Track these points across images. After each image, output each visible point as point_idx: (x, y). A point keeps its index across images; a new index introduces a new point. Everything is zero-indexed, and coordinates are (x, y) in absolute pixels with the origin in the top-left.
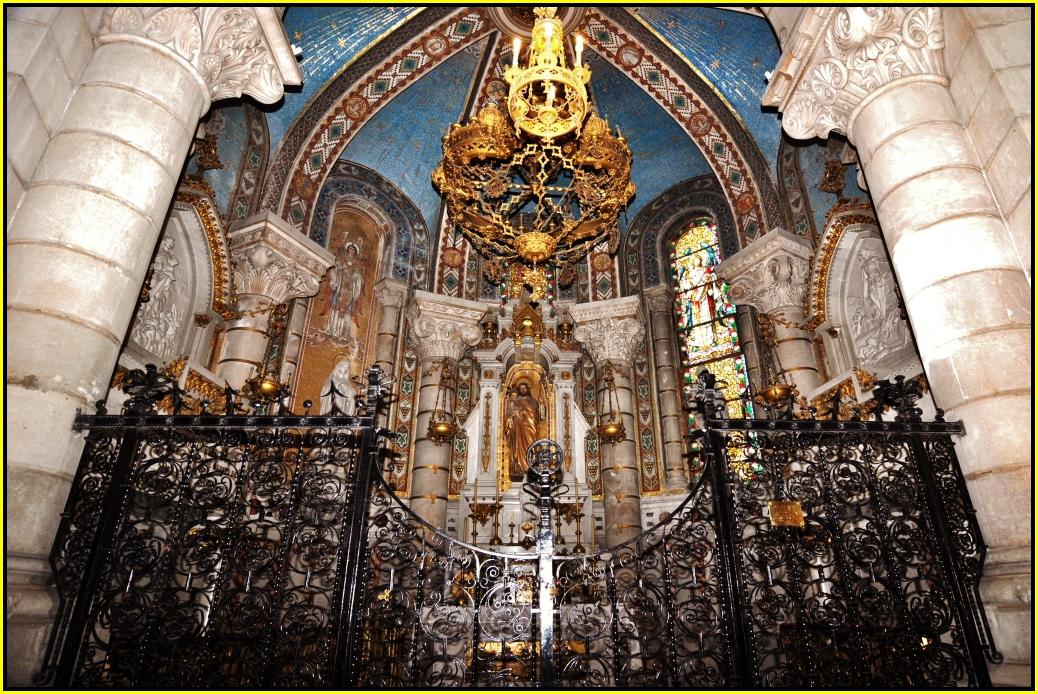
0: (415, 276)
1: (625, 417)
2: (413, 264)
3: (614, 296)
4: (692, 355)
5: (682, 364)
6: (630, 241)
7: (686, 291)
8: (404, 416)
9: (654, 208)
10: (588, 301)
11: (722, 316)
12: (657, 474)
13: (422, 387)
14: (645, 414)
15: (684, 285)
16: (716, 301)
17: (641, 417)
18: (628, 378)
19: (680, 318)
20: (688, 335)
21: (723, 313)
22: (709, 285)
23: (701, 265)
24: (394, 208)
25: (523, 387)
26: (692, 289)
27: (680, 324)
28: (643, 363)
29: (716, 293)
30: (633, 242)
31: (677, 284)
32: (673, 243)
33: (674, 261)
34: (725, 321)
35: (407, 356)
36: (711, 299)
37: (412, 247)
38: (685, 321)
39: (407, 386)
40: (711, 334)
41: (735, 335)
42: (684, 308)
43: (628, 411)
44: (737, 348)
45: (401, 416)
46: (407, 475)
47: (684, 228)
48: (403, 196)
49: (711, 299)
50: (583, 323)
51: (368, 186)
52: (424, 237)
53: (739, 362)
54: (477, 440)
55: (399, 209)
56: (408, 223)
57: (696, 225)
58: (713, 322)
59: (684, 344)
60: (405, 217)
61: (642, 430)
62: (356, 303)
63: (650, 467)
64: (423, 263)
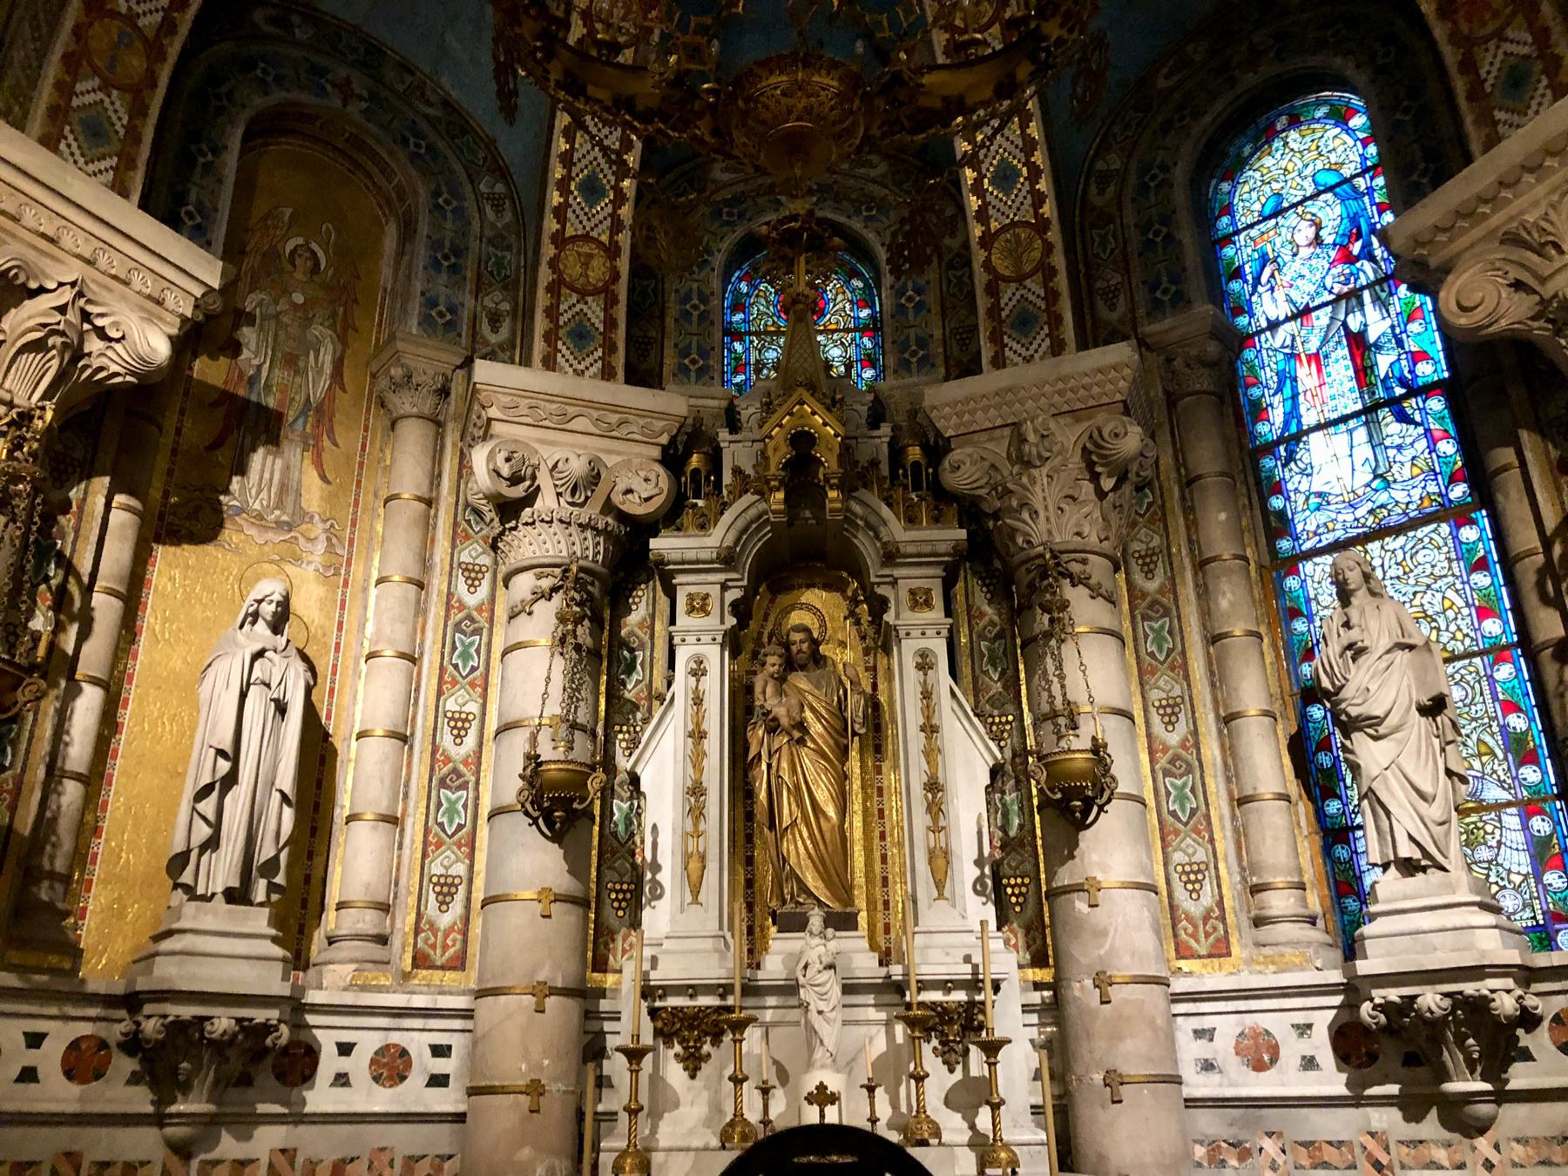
0: (485, 328)
1: (1113, 722)
2: (477, 293)
3: (1057, 348)
4: (1307, 522)
5: (1273, 551)
6: (1093, 189)
7: (1273, 325)
8: (459, 738)
9: (1161, 83)
10: (980, 371)
11: (1399, 391)
12: (1220, 903)
13: (504, 654)
14: (1170, 712)
15: (1269, 306)
16: (1378, 347)
17: (1156, 719)
18: (1111, 600)
19: (1259, 411)
20: (1291, 457)
21: (1402, 382)
22: (1352, 298)
24: (419, 135)
25: (796, 637)
26: (1293, 317)
27: (1262, 428)
28: (1151, 553)
29: (1376, 323)
30: (1101, 192)
31: (1241, 309)
32: (1225, 186)
33: (1228, 240)
34: (1411, 405)
35: (465, 557)
36: (1359, 344)
37: (474, 245)
38: (1277, 416)
39: (467, 647)
40: (1364, 451)
41: (1448, 447)
42: (1268, 376)
43: (1119, 703)
44: (1459, 491)
45: (446, 740)
46: (466, 920)
47: (1256, 139)
48: (446, 104)
49: (1359, 344)
50: (966, 436)
51: (342, 72)
52: (508, 217)
53: (1468, 534)
54: (669, 799)
55: (432, 136)
56: (464, 177)
57: (1295, 122)
58: (1369, 411)
59: (1278, 488)
60: (452, 159)
61: (1163, 761)
62: (319, 410)
63: (1194, 876)
64: (505, 288)
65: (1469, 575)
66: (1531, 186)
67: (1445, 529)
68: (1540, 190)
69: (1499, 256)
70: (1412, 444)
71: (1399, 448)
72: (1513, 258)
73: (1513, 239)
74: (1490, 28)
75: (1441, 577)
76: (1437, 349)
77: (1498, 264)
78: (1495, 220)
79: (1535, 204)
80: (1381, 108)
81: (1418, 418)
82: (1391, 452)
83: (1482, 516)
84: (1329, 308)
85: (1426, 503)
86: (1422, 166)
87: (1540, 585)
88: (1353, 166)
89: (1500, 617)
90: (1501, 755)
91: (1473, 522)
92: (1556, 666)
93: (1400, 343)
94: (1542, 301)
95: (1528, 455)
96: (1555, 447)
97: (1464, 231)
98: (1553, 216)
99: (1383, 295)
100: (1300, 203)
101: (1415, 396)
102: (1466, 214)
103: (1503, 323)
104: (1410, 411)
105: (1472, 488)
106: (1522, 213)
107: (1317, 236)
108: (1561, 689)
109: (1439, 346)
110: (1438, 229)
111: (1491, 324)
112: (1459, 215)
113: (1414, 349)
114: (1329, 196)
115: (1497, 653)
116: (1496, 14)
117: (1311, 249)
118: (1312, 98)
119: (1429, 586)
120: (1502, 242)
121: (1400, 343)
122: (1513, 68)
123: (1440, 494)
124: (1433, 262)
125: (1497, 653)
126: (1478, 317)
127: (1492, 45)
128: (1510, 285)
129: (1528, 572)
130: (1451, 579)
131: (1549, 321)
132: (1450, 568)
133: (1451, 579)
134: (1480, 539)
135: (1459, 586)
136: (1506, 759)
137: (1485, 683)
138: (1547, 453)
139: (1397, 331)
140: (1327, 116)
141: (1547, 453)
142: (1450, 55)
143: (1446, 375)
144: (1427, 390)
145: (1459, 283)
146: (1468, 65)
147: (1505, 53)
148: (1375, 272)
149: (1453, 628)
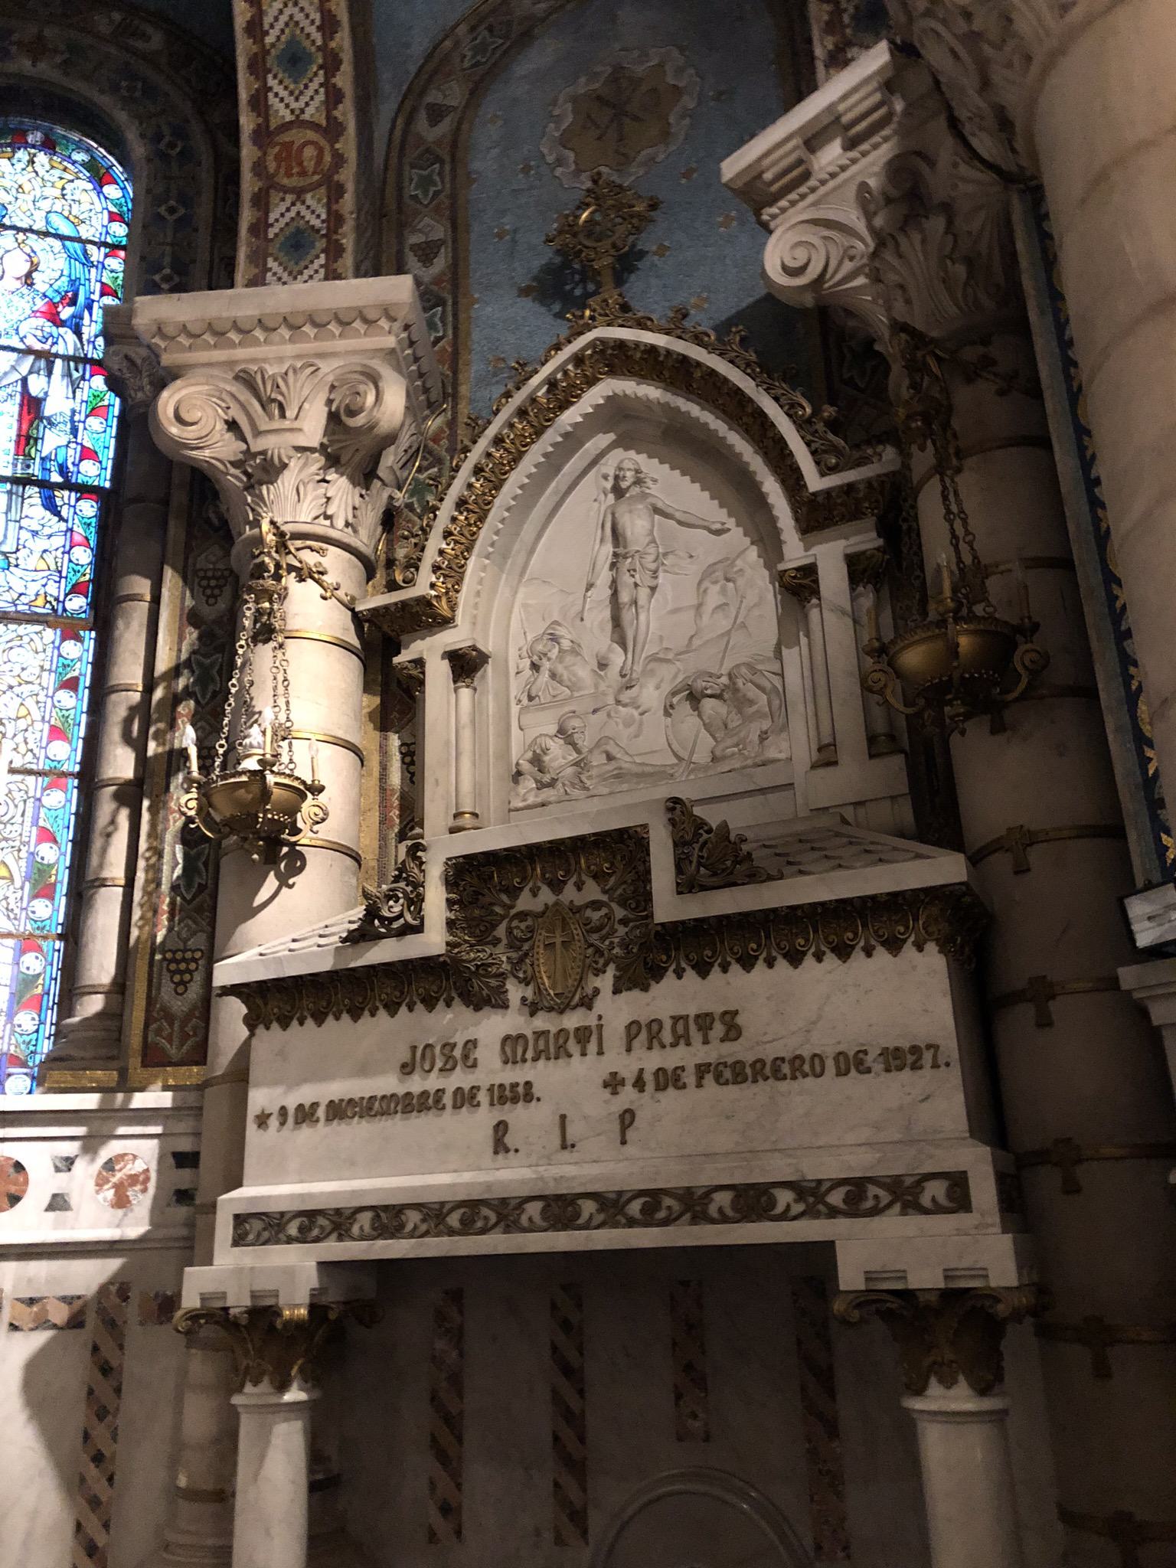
11: (56, 478)
21: (63, 470)
23: (28, 280)
29: (58, 399)
36: (32, 407)
41: (83, 556)
44: (77, 604)
53: (71, 649)
57: (49, 145)
65: (56, 690)
66: (283, 341)
67: (50, 634)
68: (290, 349)
69: (228, 388)
70: (50, 536)
71: (35, 533)
72: (238, 395)
73: (247, 380)
74: (294, 182)
75: (27, 683)
76: (108, 455)
77: (224, 396)
78: (241, 353)
79: (280, 360)
80: (149, 191)
81: (64, 513)
82: (25, 535)
83: (90, 637)
84: (15, 355)
85: (40, 601)
86: (167, 271)
87: (128, 722)
88: (92, 231)
89: (70, 743)
90: (18, 883)
91: (79, 639)
92: (113, 805)
93: (74, 431)
94: (249, 454)
95: (165, 593)
96: (193, 596)
97: (208, 347)
98: (291, 377)
99: (76, 375)
100: (24, 231)
101: (71, 490)
102: (217, 331)
103: (207, 453)
104: (59, 502)
105: (94, 605)
106: (265, 360)
107: (29, 275)
108: (110, 829)
109: (111, 454)
110: (184, 329)
111: (193, 449)
112: (210, 328)
113: (87, 444)
114: (57, 244)
115: (55, 776)
116: (303, 173)
117: (18, 284)
118: (75, 136)
119: (11, 687)
120: (237, 378)
121: (74, 431)
122: (299, 232)
123: (57, 599)
124: (166, 360)
125: (55, 776)
126: (188, 434)
127: (289, 198)
128: (226, 422)
129: (119, 706)
130: (36, 688)
131: (245, 473)
132: (40, 677)
133: (36, 688)
134: (80, 659)
135: (42, 698)
136: (22, 888)
137: (30, 803)
138: (183, 599)
139: (76, 418)
140: (84, 164)
141: (183, 599)
142: (249, 184)
143: (107, 485)
144: (84, 490)
145: (184, 392)
146: (261, 202)
147: (298, 213)
148: (76, 349)
149: (20, 738)
